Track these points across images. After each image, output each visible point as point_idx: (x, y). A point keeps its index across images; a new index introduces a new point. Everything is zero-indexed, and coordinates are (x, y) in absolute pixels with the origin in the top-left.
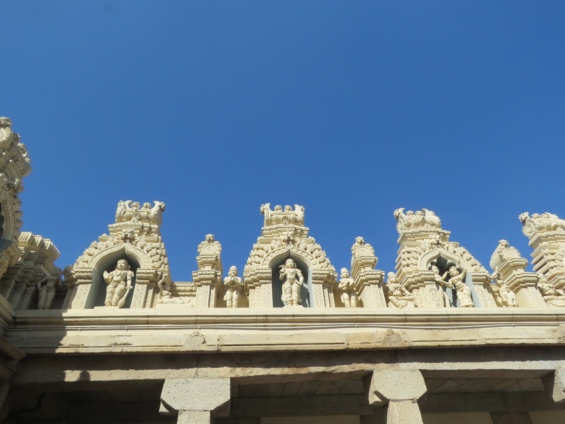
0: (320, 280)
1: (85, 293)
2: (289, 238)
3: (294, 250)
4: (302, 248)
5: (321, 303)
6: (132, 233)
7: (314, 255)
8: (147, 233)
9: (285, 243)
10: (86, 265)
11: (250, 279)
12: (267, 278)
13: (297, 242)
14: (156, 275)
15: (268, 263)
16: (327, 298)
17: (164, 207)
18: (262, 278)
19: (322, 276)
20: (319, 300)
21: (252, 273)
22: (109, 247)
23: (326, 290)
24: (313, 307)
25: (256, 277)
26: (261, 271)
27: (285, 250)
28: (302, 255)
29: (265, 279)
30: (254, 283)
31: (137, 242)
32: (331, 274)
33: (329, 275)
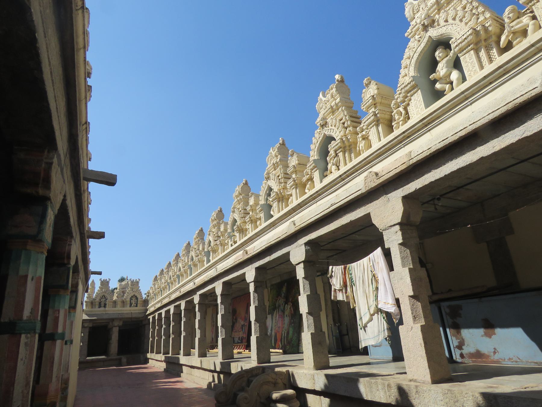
0: (467, 47)
2: (423, 25)
4: (442, 23)
12: (413, 87)
17: (342, 77)
18: (408, 92)
30: (406, 99)
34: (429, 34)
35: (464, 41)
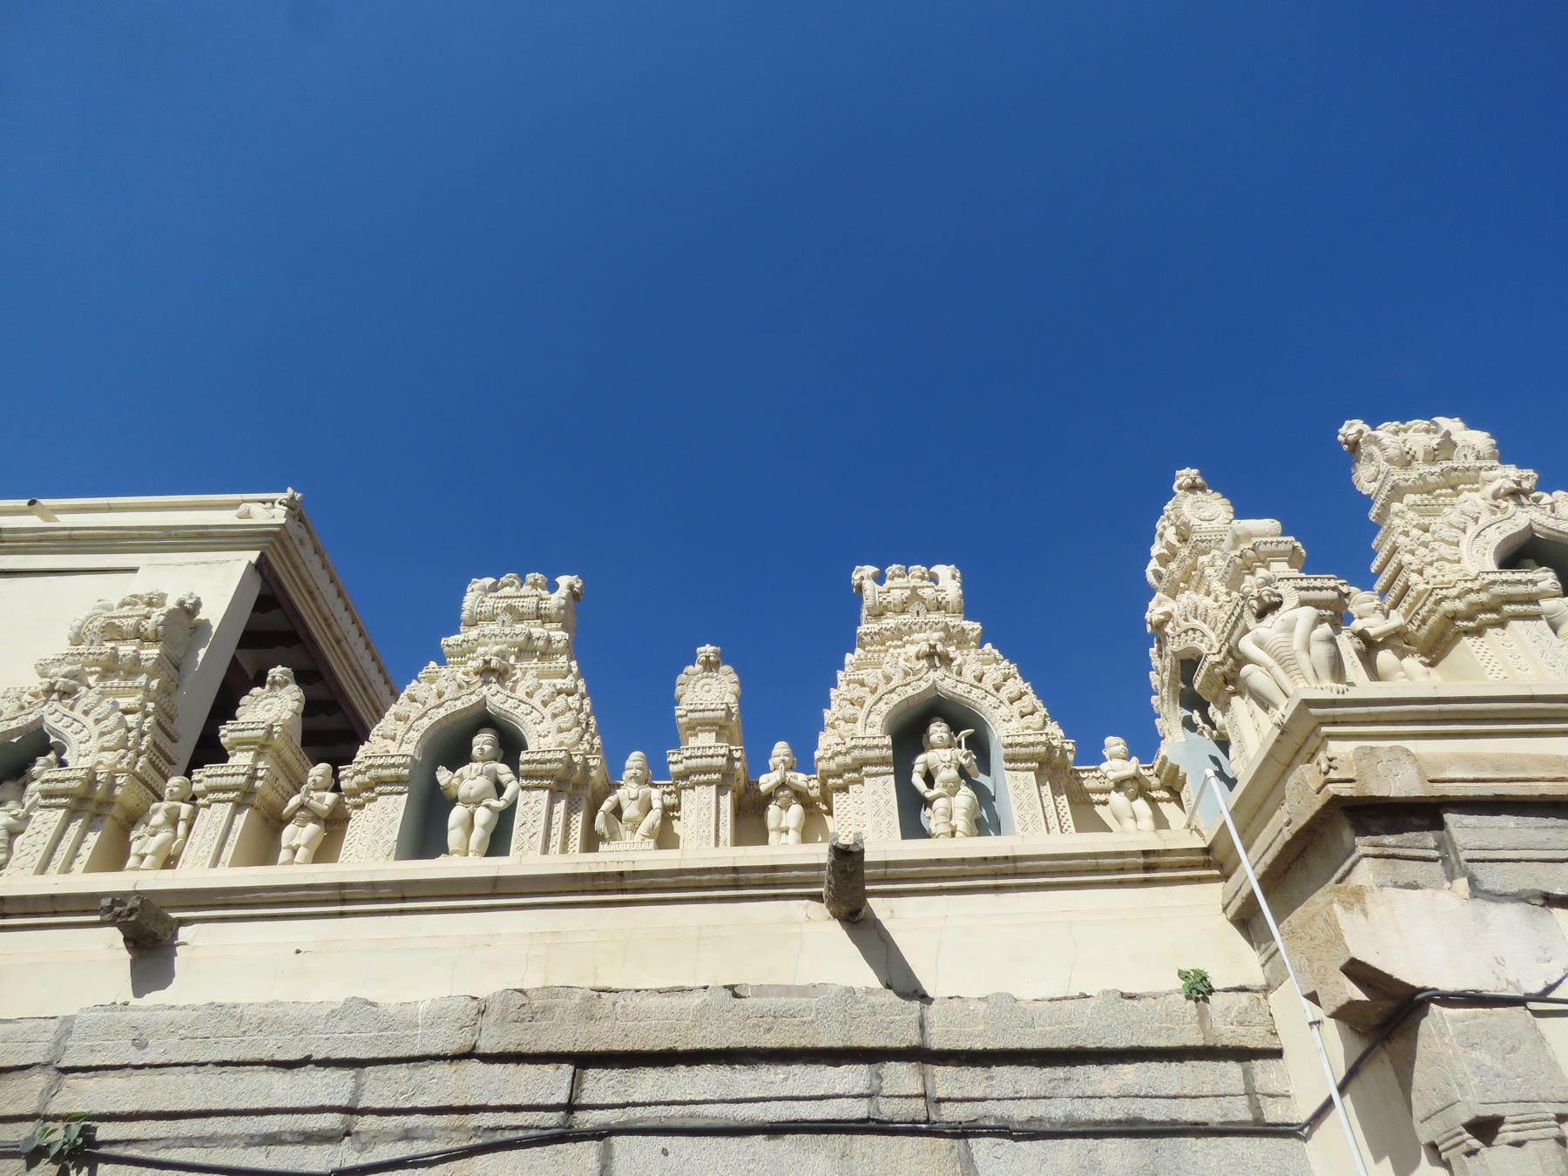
0: (1026, 761)
1: (392, 821)
2: (934, 647)
3: (947, 683)
4: (968, 675)
5: (1033, 822)
6: (502, 655)
7: (1004, 694)
8: (543, 654)
9: (924, 662)
10: (393, 747)
11: (832, 765)
12: (882, 761)
13: (952, 660)
14: (570, 765)
15: (877, 719)
16: (1051, 809)
18: (867, 762)
19: (1031, 749)
20: (1028, 818)
21: (839, 748)
22: (445, 697)
23: (1047, 789)
24: (1012, 832)
25: (848, 759)
26: (864, 743)
27: (924, 685)
28: (971, 696)
29: (876, 765)
30: (846, 776)
31: (516, 682)
32: (1055, 743)
33: (1050, 748)
34: (933, 675)
35: (1026, 746)
